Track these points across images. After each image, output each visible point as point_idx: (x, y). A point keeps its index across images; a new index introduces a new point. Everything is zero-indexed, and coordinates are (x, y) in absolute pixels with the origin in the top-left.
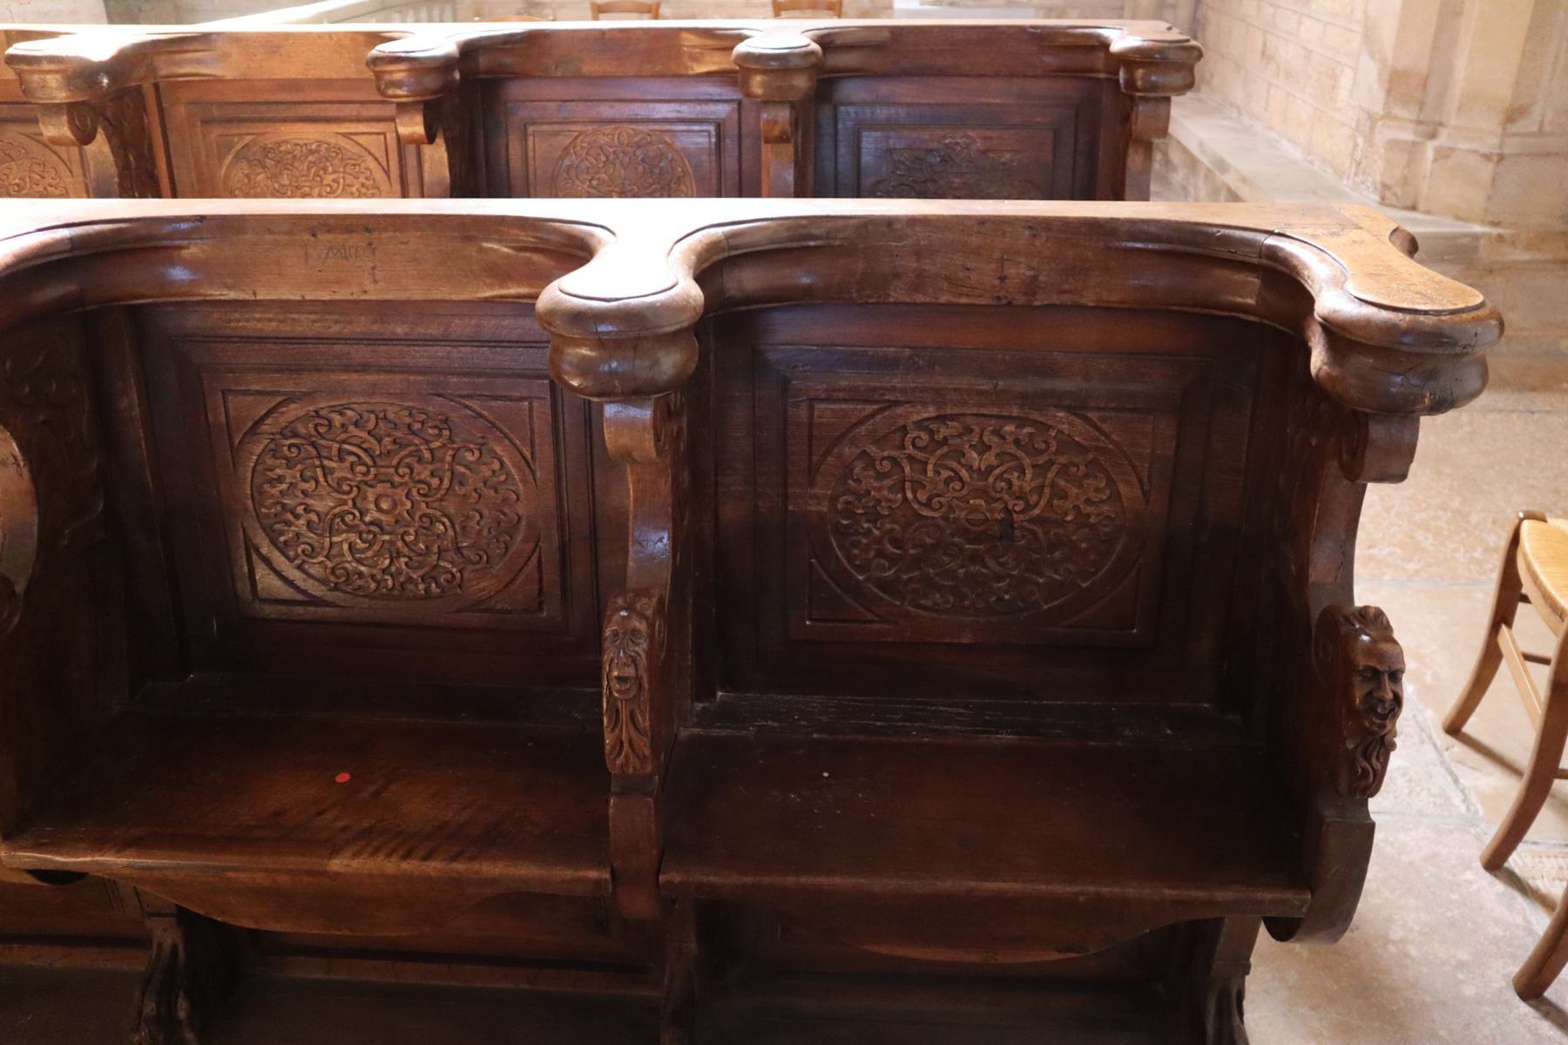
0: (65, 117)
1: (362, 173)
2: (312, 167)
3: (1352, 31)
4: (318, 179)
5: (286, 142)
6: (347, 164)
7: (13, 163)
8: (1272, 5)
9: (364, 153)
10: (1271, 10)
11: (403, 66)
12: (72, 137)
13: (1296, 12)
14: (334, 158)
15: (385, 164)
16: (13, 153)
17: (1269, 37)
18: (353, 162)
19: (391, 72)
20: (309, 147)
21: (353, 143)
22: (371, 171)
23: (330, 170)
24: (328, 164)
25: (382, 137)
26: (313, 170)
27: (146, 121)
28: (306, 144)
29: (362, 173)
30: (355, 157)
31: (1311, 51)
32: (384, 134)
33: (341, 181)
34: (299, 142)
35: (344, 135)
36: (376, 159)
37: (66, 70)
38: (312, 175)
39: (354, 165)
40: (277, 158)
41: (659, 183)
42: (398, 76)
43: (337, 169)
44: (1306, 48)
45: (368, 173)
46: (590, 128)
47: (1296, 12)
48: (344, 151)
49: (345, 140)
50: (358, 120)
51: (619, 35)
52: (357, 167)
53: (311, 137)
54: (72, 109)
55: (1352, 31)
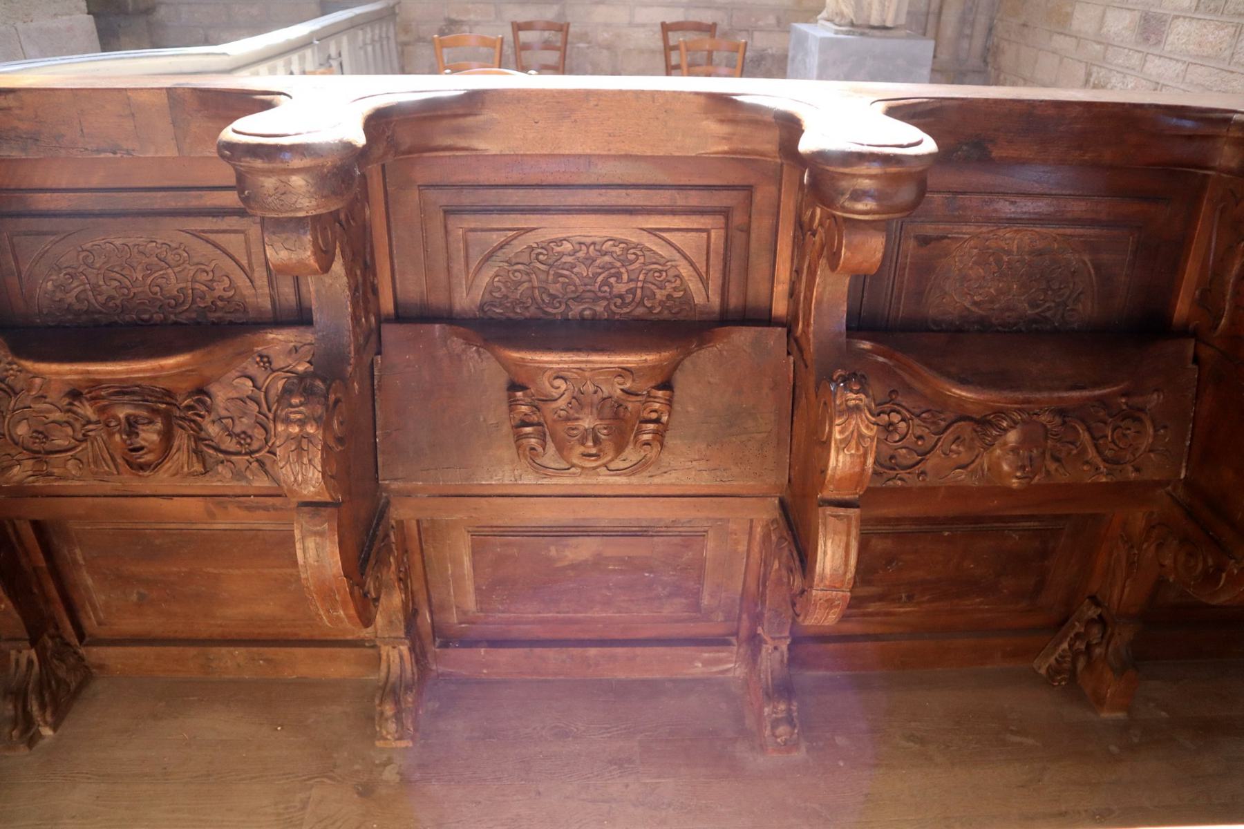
0: (309, 237)
1: (669, 281)
2: (600, 274)
3: (1232, 72)
4: (606, 288)
5: (559, 242)
6: (651, 270)
7: (170, 271)
8: (1099, 43)
9: (677, 256)
10: (1098, 47)
11: (863, 169)
12: (317, 266)
13: (1139, 52)
14: (632, 262)
15: (703, 270)
16: (170, 258)
17: (1095, 69)
18: (660, 267)
19: (854, 176)
20: (597, 247)
21: (663, 243)
22: (681, 280)
23: (625, 277)
24: (623, 270)
25: (704, 235)
26: (600, 279)
27: (368, 213)
28: (594, 243)
29: (669, 281)
30: (662, 261)
31: (1164, 85)
32: (707, 231)
33: (639, 291)
34: (583, 240)
35: (651, 231)
36: (692, 264)
37: (323, 166)
38: (597, 285)
39: (660, 271)
40: (550, 261)
41: (1054, 301)
42: (866, 184)
43: (633, 277)
44: (1158, 83)
45: (678, 282)
46: (984, 229)
47: (1139, 52)
48: (647, 253)
49: (653, 238)
50: (673, 212)
51: (1051, 111)
52: (664, 274)
53: (604, 234)
54: (316, 222)
55: (1232, 72)
